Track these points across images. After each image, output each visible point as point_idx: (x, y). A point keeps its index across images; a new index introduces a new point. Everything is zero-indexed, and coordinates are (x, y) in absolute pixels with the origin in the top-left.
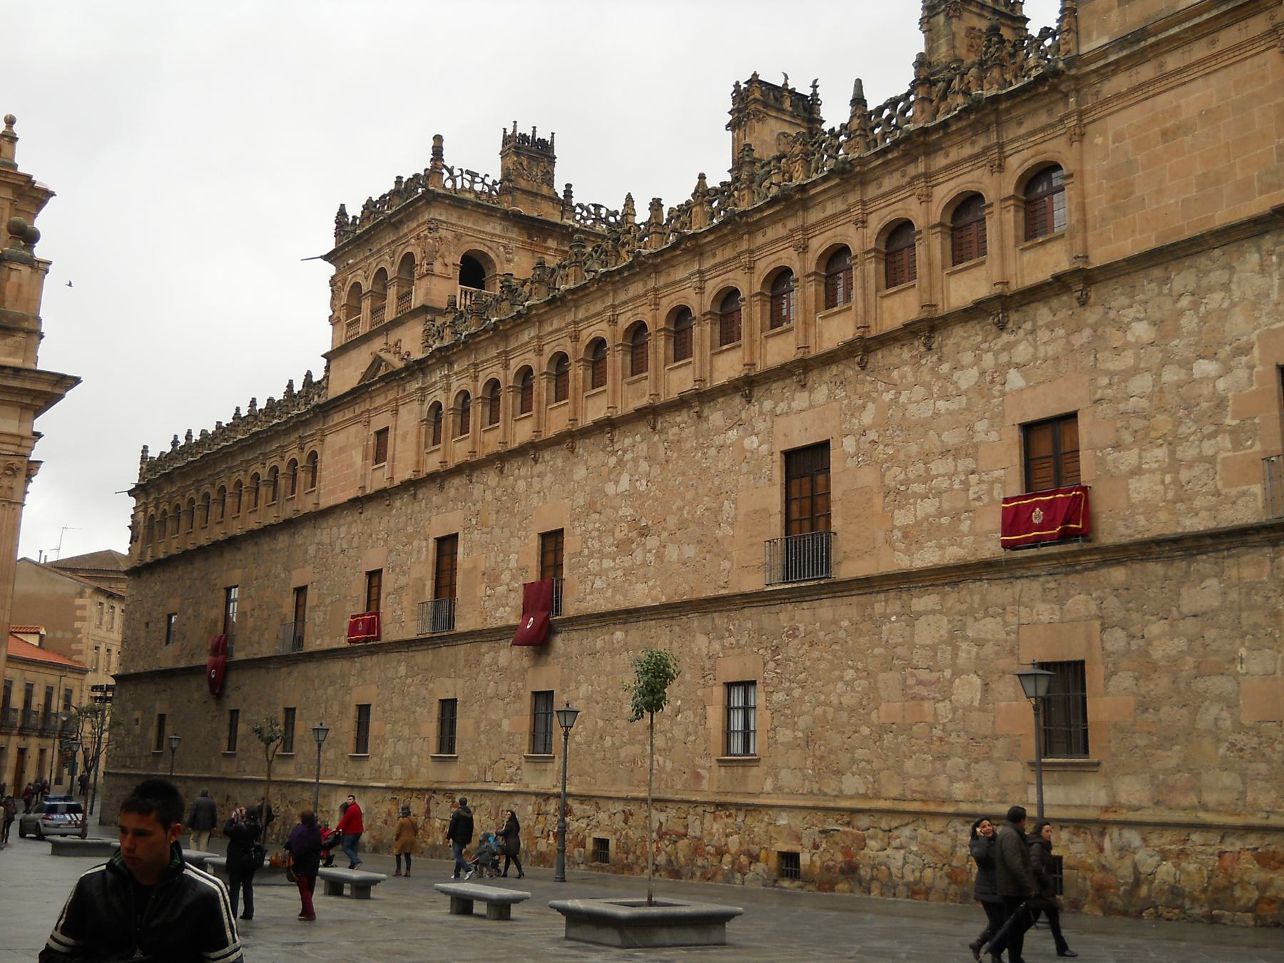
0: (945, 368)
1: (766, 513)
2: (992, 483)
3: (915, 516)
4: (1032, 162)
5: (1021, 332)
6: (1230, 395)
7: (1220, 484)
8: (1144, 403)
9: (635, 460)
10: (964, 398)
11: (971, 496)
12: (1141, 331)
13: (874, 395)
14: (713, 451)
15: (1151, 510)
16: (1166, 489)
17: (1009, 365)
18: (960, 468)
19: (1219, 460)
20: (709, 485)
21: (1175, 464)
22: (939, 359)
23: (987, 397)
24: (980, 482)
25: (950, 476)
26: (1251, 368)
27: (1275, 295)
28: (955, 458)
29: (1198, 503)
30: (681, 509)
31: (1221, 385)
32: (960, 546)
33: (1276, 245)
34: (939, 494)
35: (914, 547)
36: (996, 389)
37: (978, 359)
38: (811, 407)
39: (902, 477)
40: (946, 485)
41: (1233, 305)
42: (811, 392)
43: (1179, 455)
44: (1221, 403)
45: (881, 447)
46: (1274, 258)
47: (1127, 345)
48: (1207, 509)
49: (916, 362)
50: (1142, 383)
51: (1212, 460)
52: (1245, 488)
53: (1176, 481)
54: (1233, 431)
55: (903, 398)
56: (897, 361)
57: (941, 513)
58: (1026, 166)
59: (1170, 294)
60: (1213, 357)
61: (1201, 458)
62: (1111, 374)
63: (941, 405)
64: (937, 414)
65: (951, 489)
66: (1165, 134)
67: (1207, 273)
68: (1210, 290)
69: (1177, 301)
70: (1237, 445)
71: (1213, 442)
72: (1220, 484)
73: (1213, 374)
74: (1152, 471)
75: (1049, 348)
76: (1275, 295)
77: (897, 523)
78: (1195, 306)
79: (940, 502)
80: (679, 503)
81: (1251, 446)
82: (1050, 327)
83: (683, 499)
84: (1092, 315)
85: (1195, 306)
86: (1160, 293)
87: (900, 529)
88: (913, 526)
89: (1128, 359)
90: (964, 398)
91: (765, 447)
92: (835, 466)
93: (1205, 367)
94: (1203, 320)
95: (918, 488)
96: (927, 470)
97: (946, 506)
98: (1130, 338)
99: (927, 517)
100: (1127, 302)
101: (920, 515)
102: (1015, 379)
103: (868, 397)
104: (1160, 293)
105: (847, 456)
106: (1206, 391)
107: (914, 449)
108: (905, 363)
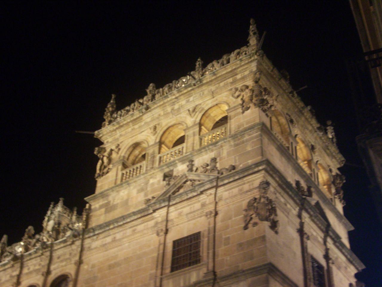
4: (59, 274)
66: (110, 267)
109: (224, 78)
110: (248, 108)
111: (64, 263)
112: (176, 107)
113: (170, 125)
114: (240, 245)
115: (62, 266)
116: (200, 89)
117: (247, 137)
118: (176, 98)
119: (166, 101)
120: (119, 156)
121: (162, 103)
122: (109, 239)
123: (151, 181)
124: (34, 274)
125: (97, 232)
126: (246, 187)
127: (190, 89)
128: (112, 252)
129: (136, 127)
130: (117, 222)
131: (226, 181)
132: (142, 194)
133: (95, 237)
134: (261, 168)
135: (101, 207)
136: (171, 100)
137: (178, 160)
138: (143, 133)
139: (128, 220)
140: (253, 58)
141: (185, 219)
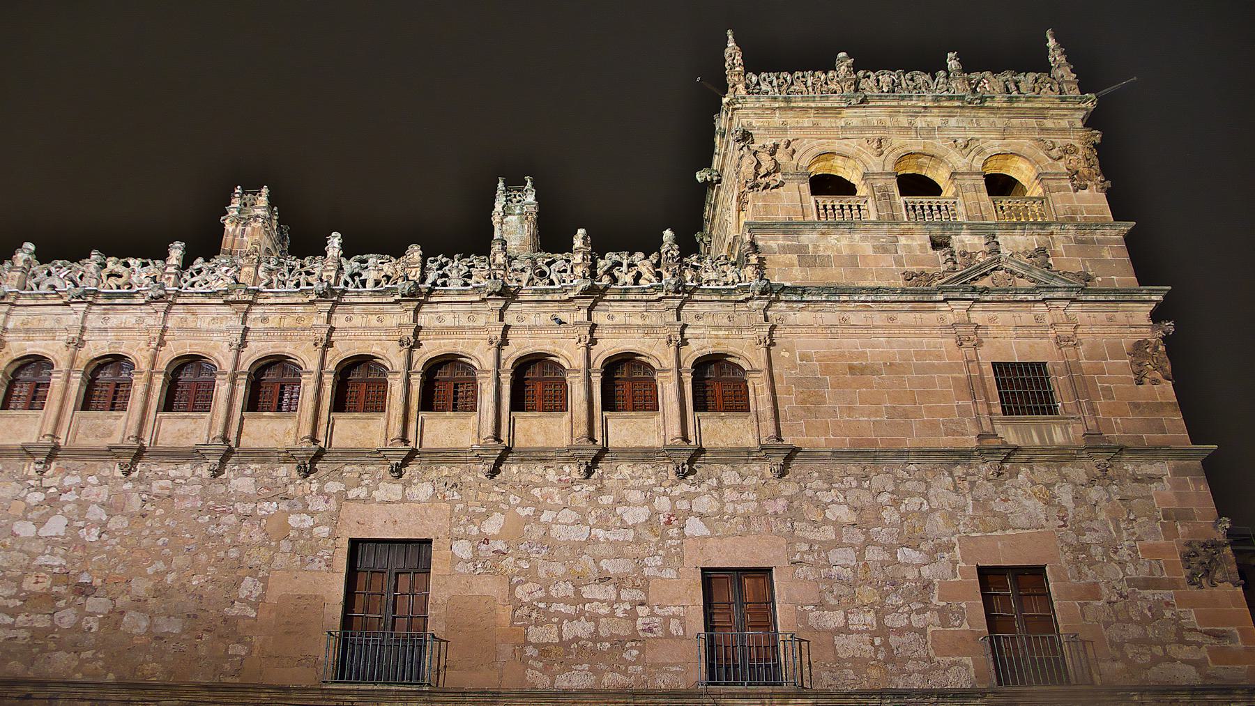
0: (606, 500)
1: (317, 601)
2: (667, 619)
3: (560, 636)
4: (711, 350)
5: (704, 487)
6: (935, 581)
7: (932, 653)
8: (848, 573)
9: (83, 506)
10: (631, 533)
11: (639, 626)
12: (842, 513)
13: (505, 507)
14: (233, 519)
15: (859, 664)
16: (876, 653)
17: (690, 512)
18: (625, 595)
19: (929, 631)
20: (222, 554)
21: (882, 630)
22: (598, 490)
23: (664, 537)
24: (652, 614)
25: (611, 604)
26: (955, 563)
27: (970, 511)
28: (619, 587)
29: (910, 666)
30: (160, 575)
31: (926, 572)
32: (625, 673)
33: (967, 474)
34: (595, 618)
35: (557, 667)
36: (674, 532)
37: (649, 502)
38: (404, 500)
39: (540, 594)
40: (605, 610)
41: (932, 511)
42: (408, 484)
43: (889, 621)
44: (928, 586)
45: (511, 559)
46: (966, 483)
47: (826, 521)
48: (919, 672)
49: (567, 486)
50: (842, 558)
51: (923, 631)
52: (957, 659)
53: (886, 644)
54: (941, 611)
55: (546, 517)
56: (538, 480)
57: (596, 638)
58: (706, 352)
59: (870, 488)
60: (916, 548)
61: (910, 628)
62: (806, 541)
63: (600, 533)
64: (592, 541)
65: (612, 614)
66: (852, 369)
67: (904, 481)
68: (909, 494)
69: (875, 497)
70: (945, 622)
71: (921, 616)
72: (932, 653)
73: (918, 561)
74: (858, 632)
75: (739, 507)
76: (970, 511)
77: (532, 639)
78: (896, 503)
79: (597, 627)
80: (160, 566)
81: (960, 625)
82: (740, 489)
83: (168, 561)
84: (788, 488)
85: (896, 503)
86: (859, 487)
87: (535, 646)
88: (556, 645)
89: (829, 533)
90: (631, 533)
91: (323, 531)
92: (437, 567)
93: (904, 554)
94: (904, 516)
95: (562, 608)
96: (578, 592)
97: (603, 632)
98: (829, 514)
99: (577, 639)
100: (826, 486)
101: (567, 635)
102: (695, 527)
103: (492, 508)
104: (859, 487)
105: (455, 560)
106: (911, 574)
107: (559, 569)
108: (546, 483)
109: (1023, 114)
110: (1085, 187)
111: (721, 333)
112: (920, 122)
113: (914, 149)
114: (1136, 406)
115: (717, 337)
116: (973, 112)
117: (1097, 236)
118: (925, 108)
119: (902, 103)
120: (794, 162)
121: (894, 103)
122: (830, 318)
123: (903, 240)
124: (638, 334)
125: (806, 298)
126: (1120, 317)
127: (957, 104)
128: (850, 344)
129: (825, 122)
130: (850, 294)
131: (1093, 298)
132: (890, 258)
133: (801, 305)
134: (1154, 298)
135: (784, 250)
136: (913, 106)
137: (968, 225)
138: (846, 141)
139: (886, 298)
140: (1084, 106)
141: (1013, 333)
